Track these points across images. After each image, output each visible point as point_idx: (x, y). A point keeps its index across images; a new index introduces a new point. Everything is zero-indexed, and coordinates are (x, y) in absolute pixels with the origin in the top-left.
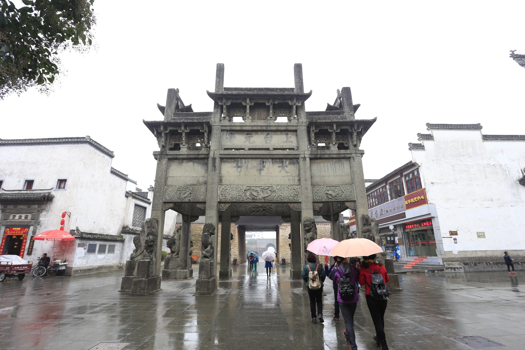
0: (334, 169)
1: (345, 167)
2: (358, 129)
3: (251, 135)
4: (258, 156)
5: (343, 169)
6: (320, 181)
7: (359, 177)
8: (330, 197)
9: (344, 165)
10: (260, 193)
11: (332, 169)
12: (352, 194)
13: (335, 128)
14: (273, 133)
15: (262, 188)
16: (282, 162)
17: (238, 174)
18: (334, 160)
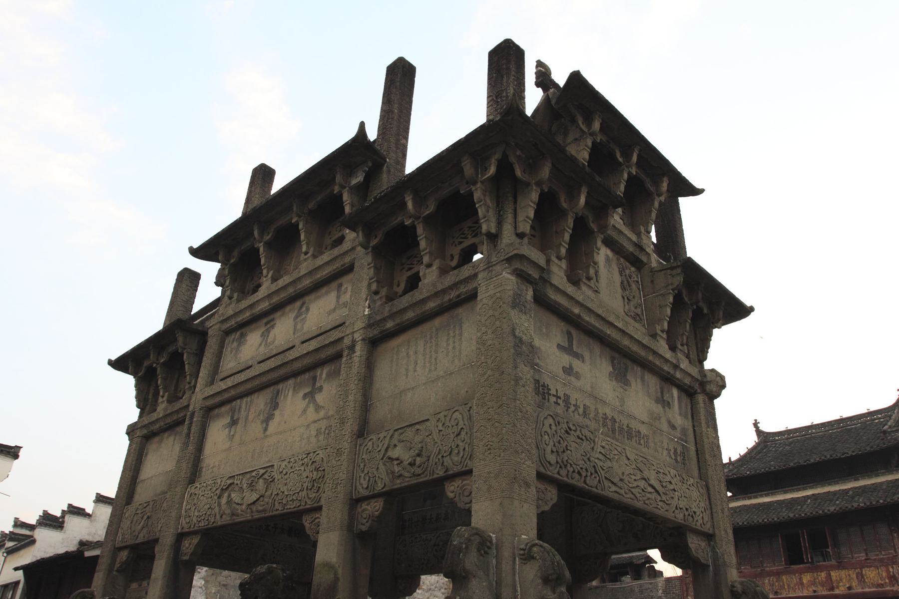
0: (431, 357)
1: (466, 335)
2: (486, 169)
3: (272, 323)
4: (264, 379)
5: (457, 345)
6: (389, 416)
7: (489, 361)
8: (396, 469)
9: (464, 328)
10: (247, 494)
11: (427, 360)
12: (461, 444)
13: (410, 205)
14: (312, 296)
15: (254, 474)
16: (314, 379)
17: (228, 445)
18: (437, 322)
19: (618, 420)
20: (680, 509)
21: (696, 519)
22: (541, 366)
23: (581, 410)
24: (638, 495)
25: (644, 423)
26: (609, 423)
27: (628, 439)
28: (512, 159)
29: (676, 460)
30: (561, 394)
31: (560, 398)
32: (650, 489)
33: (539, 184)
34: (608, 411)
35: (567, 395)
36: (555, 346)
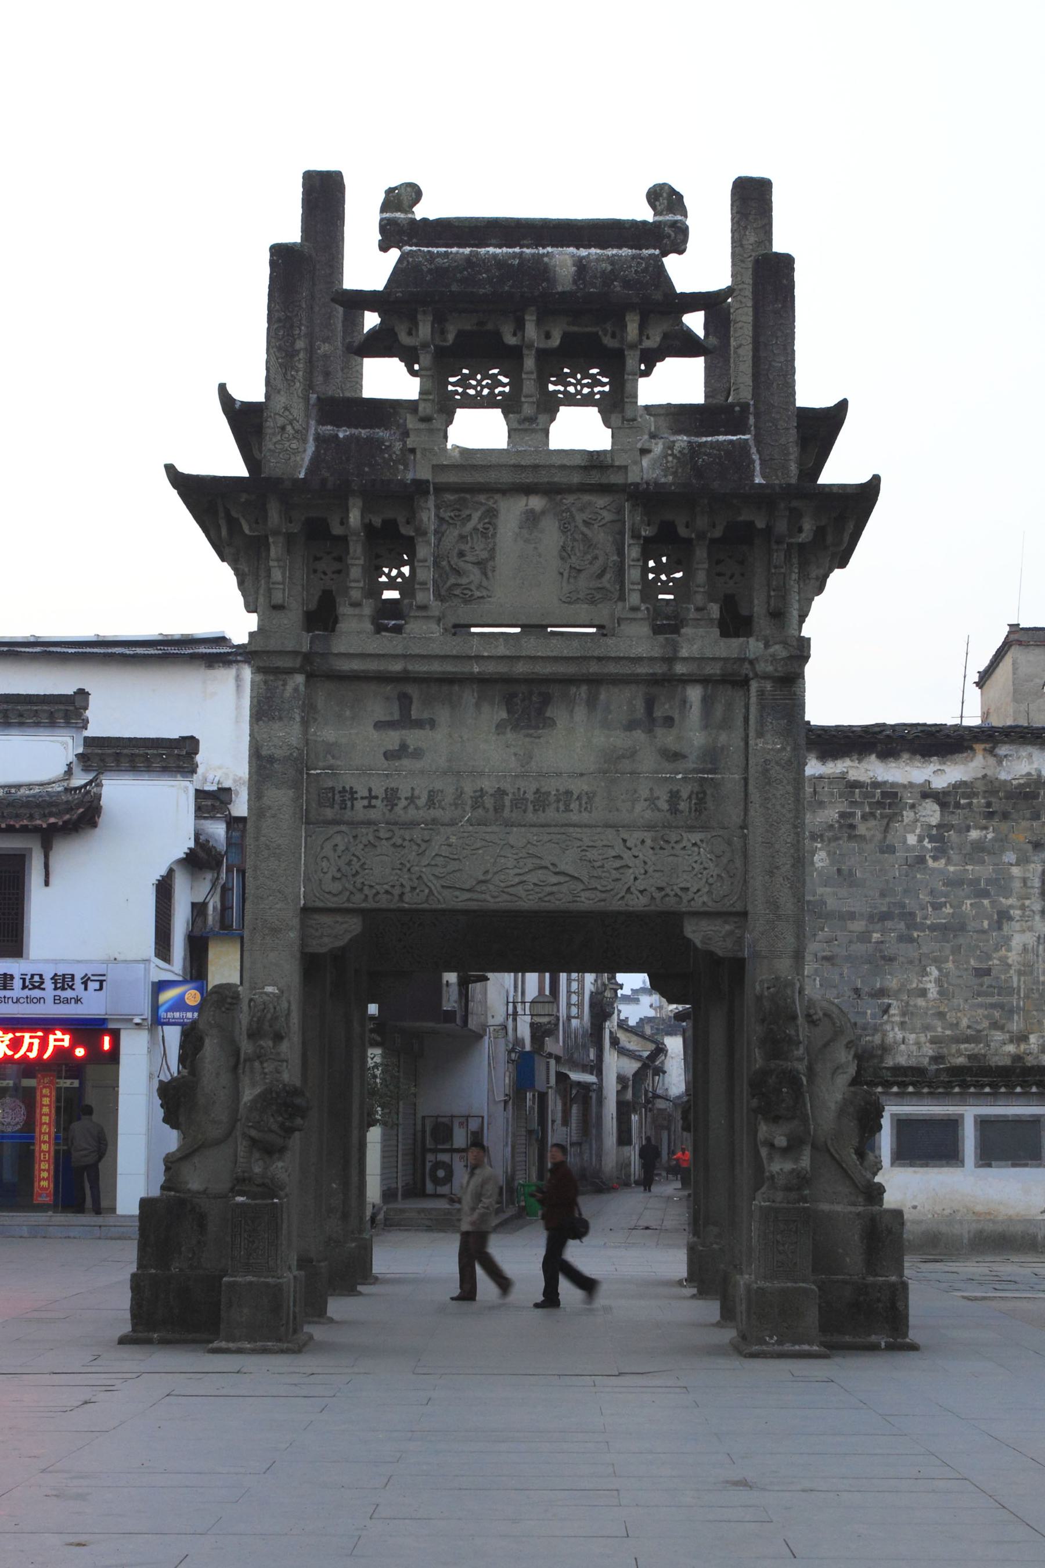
19: (510, 790)
20: (641, 892)
21: (685, 898)
22: (338, 766)
23: (422, 801)
24: (523, 894)
25: (582, 775)
26: (489, 802)
27: (535, 811)
28: (234, 514)
29: (674, 810)
30: (379, 790)
31: (376, 797)
32: (554, 879)
33: (276, 533)
34: (488, 785)
35: (392, 789)
36: (371, 729)
